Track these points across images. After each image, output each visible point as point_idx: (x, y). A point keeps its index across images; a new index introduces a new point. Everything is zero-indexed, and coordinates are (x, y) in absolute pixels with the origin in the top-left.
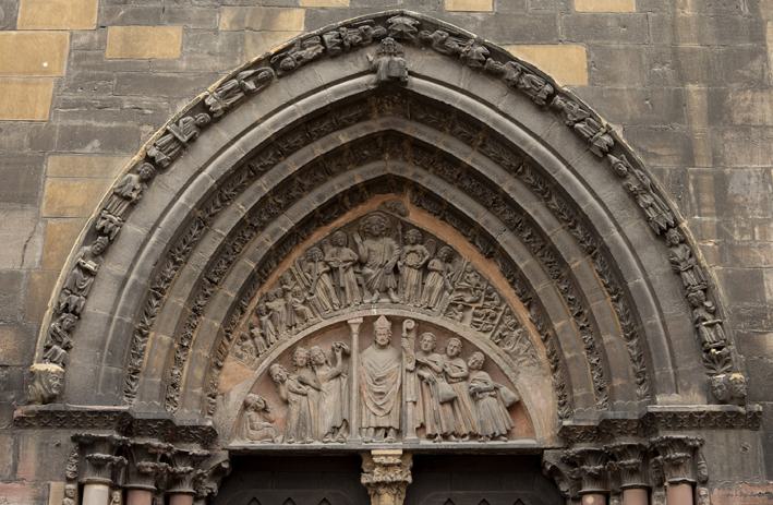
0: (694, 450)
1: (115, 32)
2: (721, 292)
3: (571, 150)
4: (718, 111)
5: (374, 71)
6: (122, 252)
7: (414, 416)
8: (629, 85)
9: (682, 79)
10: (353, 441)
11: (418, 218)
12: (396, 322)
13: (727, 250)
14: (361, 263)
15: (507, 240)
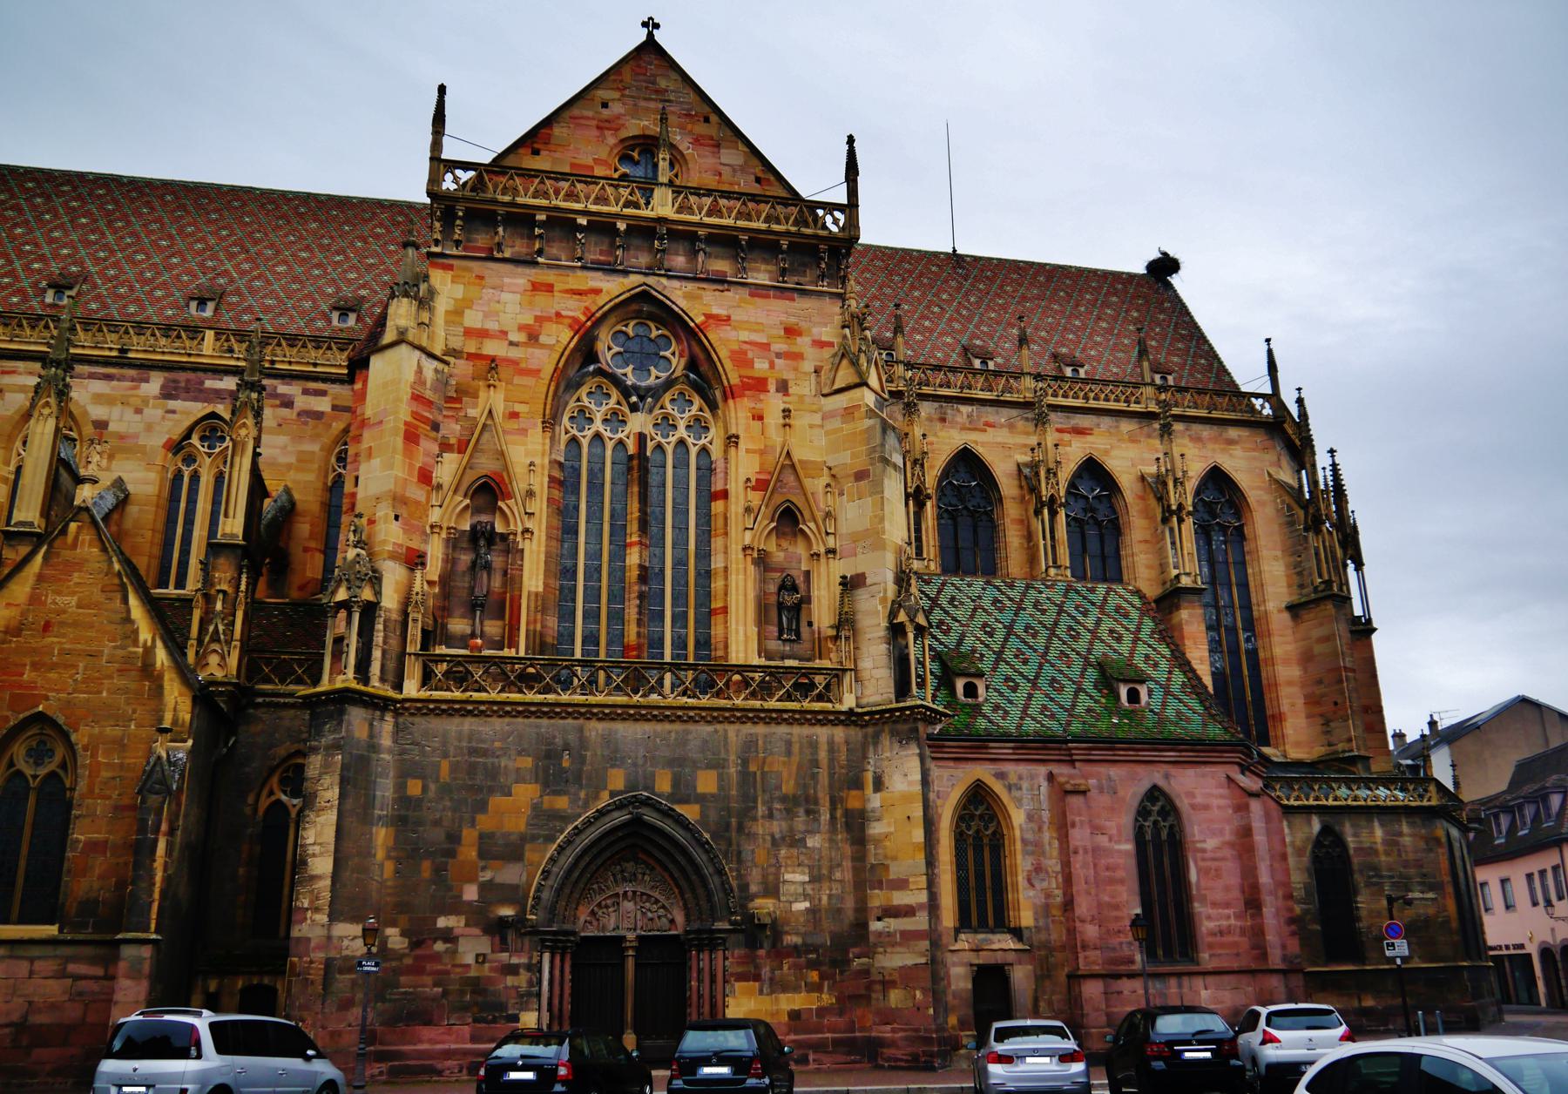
0: (724, 940)
1: (546, 798)
2: (736, 890)
3: (694, 843)
4: (740, 828)
5: (631, 813)
6: (552, 877)
7: (639, 924)
8: (713, 816)
9: (730, 817)
10: (621, 933)
11: (640, 855)
12: (634, 892)
13: (740, 877)
14: (622, 871)
15: (671, 866)
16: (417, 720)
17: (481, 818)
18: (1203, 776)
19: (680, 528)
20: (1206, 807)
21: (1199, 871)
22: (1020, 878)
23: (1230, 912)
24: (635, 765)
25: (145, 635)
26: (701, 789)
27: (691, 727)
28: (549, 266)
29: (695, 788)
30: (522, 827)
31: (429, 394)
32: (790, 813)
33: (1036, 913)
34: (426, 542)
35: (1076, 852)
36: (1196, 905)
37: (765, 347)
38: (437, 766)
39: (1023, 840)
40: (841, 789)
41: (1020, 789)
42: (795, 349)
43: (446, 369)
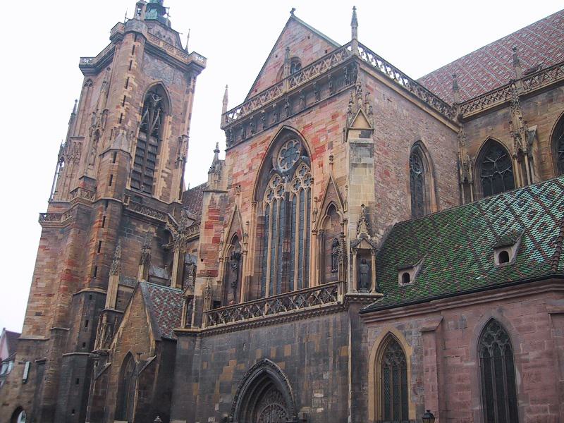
16: (207, 338)
17: (221, 376)
18: (528, 306)
19: (300, 230)
20: (530, 328)
21: (523, 375)
22: (409, 390)
23: (547, 405)
24: (265, 346)
25: (148, 321)
26: (285, 355)
27: (284, 325)
28: (255, 136)
29: (283, 354)
30: (231, 378)
31: (217, 207)
32: (317, 362)
33: (417, 411)
34: (218, 266)
35: (427, 371)
36: (520, 401)
37: (324, 130)
38: (211, 356)
39: (411, 365)
40: (338, 347)
41: (411, 334)
42: (335, 125)
43: (227, 195)
